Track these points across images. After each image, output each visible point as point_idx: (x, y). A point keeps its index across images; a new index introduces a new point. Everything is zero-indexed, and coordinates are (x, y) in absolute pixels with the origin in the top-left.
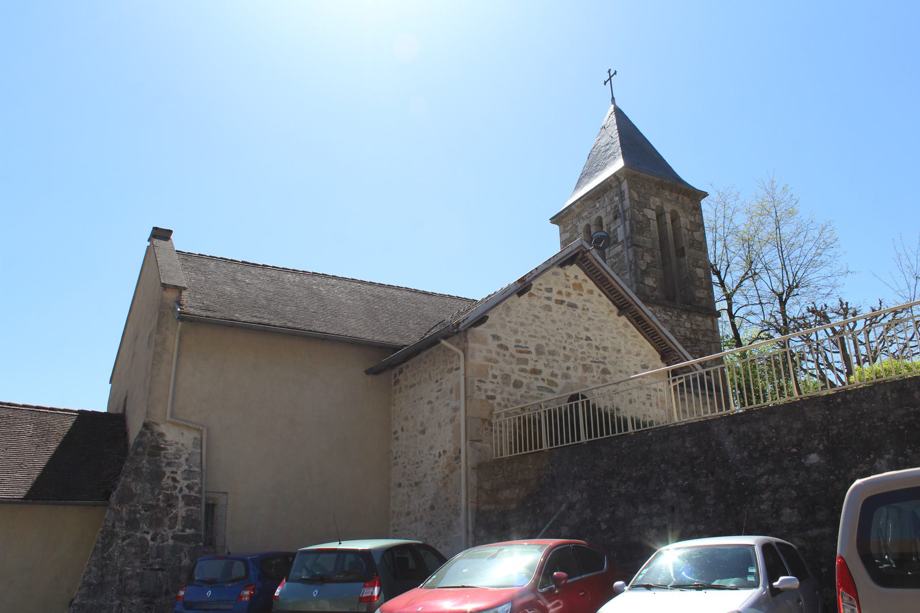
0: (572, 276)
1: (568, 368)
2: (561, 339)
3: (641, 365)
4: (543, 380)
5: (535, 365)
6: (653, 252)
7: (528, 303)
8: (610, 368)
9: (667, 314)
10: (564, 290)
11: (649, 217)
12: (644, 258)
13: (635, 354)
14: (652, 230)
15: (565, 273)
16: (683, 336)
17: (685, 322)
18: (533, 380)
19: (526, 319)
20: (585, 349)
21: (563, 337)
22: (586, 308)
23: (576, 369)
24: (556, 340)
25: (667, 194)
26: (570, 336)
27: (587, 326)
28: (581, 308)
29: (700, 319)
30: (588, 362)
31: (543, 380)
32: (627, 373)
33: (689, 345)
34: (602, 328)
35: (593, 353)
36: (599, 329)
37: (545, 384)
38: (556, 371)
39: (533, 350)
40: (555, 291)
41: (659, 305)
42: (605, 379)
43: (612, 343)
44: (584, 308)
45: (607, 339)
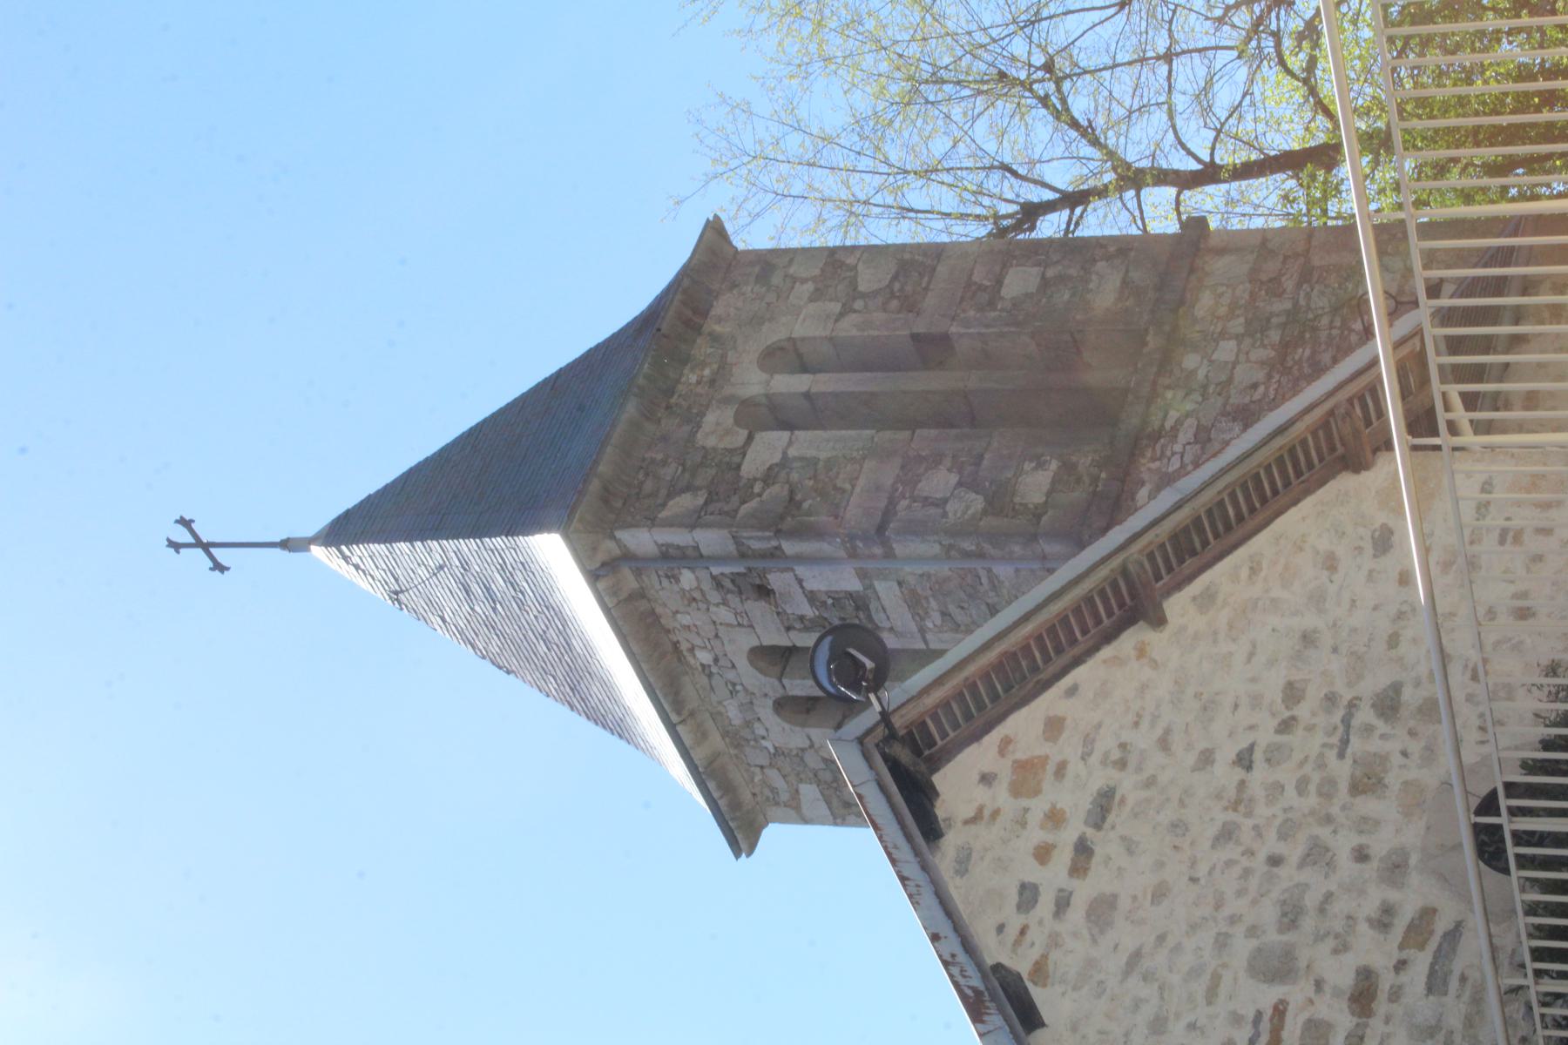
0: (981, 795)
1: (1361, 856)
2: (1236, 871)
3: (1375, 556)
4: (1401, 965)
5: (1337, 992)
7: (1075, 988)
8: (1375, 681)
10: (1037, 835)
13: (1326, 573)
15: (966, 822)
16: (1269, 377)
17: (1211, 362)
18: (1398, 1009)
19: (1137, 1005)
20: (1286, 774)
21: (1230, 863)
22: (1116, 755)
23: (1366, 824)
24: (1240, 893)
25: (693, 378)
26: (1227, 834)
27: (1191, 759)
28: (1114, 774)
29: (1205, 302)
30: (1342, 771)
31: (1401, 965)
32: (1400, 615)
33: (1308, 352)
34: (1205, 697)
35: (1306, 744)
36: (1208, 708)
37: (1421, 962)
38: (1370, 906)
39: (1268, 996)
40: (1032, 872)
42: (1420, 710)
43: (1272, 663)
44: (1115, 763)
45: (1254, 680)
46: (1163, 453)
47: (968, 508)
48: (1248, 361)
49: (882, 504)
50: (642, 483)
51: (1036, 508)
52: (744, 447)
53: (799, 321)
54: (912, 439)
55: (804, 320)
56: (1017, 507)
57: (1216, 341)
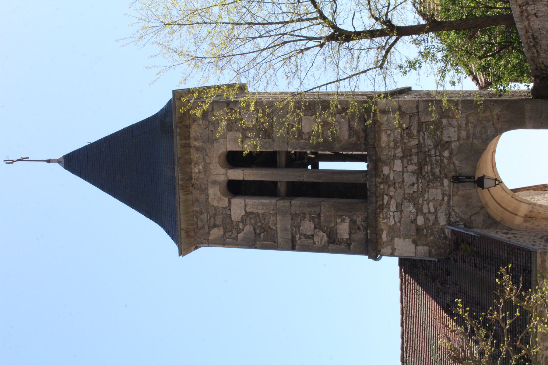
6: (296, 214)
9: (388, 204)
11: (243, 213)
12: (309, 233)
16: (418, 180)
17: (394, 171)
25: (197, 171)
29: (384, 138)
33: (429, 168)
41: (376, 221)
47: (322, 240)
48: (407, 172)
49: (290, 237)
50: (197, 222)
51: (347, 241)
54: (291, 206)
55: (229, 141)
56: (340, 240)
57: (393, 160)
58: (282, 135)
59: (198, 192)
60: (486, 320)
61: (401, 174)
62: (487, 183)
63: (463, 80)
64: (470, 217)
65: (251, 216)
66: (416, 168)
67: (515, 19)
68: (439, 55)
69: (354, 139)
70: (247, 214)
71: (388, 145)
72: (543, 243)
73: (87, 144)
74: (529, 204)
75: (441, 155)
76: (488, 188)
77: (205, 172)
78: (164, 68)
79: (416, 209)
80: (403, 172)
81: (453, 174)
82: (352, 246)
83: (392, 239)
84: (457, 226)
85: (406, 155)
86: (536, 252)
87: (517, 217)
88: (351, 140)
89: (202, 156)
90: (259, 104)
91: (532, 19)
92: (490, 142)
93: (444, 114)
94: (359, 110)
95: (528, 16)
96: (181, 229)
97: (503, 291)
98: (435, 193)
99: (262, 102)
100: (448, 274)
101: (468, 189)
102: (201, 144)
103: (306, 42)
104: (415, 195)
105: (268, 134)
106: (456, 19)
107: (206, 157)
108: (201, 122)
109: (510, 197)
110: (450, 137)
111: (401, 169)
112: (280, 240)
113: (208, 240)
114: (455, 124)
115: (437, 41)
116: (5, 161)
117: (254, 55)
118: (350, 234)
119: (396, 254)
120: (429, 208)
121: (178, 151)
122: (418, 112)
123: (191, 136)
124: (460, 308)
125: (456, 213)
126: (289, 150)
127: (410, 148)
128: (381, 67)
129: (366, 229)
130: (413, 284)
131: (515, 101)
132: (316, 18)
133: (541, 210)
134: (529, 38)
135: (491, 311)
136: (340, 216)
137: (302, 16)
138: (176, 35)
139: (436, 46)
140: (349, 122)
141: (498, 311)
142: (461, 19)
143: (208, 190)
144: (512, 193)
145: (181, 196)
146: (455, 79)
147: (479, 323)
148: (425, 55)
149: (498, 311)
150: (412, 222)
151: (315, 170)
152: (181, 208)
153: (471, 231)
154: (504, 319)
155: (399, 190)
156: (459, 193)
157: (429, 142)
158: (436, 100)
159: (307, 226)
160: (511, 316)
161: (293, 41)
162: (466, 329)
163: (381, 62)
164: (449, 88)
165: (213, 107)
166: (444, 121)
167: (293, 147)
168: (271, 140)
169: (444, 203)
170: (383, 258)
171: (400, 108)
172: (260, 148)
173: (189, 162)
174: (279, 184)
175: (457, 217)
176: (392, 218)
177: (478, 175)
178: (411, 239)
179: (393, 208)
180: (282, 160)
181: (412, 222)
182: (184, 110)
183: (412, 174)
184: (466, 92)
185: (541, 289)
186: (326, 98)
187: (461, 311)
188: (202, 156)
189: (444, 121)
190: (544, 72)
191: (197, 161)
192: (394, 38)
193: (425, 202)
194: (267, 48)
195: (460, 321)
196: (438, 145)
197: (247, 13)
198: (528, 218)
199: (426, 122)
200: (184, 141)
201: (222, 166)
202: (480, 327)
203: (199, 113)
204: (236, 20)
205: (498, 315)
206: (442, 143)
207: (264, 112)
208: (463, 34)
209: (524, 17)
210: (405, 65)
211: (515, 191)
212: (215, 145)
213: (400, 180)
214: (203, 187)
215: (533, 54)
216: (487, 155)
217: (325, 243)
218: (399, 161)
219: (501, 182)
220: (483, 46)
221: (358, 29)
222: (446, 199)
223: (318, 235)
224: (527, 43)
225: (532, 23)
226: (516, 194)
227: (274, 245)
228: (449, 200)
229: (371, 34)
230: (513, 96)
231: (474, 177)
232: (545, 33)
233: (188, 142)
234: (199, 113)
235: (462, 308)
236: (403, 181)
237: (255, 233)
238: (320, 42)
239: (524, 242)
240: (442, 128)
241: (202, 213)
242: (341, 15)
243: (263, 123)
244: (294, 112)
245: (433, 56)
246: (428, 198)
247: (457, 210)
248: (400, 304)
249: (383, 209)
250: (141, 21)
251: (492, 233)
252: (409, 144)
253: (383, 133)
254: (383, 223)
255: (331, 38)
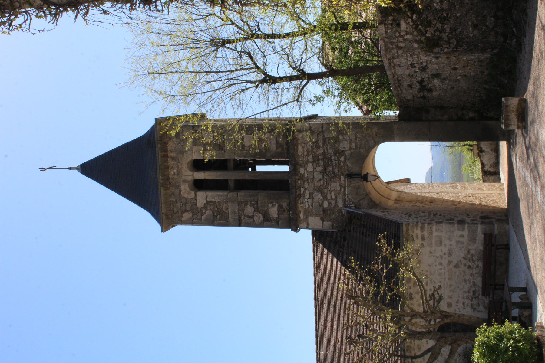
6: (241, 201)
9: (304, 193)
11: (205, 202)
14: (218, 200)
16: (323, 177)
25: (173, 173)
29: (300, 149)
33: (331, 169)
46: (303, 202)
50: (173, 208)
51: (276, 219)
52: (195, 197)
53: (193, 153)
54: (238, 196)
55: (194, 153)
57: (307, 164)
58: (230, 148)
59: (174, 188)
60: (370, 270)
61: (312, 173)
62: (370, 178)
63: (353, 109)
64: (359, 202)
65: (211, 204)
66: (322, 169)
67: (386, 68)
68: (336, 93)
69: (280, 150)
70: (208, 202)
71: (303, 154)
72: (407, 218)
73: (96, 156)
74: (398, 192)
75: (339, 160)
76: (370, 182)
77: (178, 174)
78: (149, 103)
79: (323, 197)
80: (313, 172)
81: (347, 172)
82: (280, 223)
83: (307, 218)
84: (350, 207)
85: (315, 161)
86: (402, 223)
87: (390, 201)
88: (278, 150)
89: (176, 163)
90: (214, 127)
91: (397, 68)
92: (371, 151)
93: (340, 132)
94: (283, 130)
95: (394, 66)
96: (162, 214)
97: (381, 251)
98: (335, 186)
99: (217, 125)
100: (345, 240)
101: (357, 182)
102: (175, 155)
103: (246, 84)
104: (321, 187)
105: (221, 147)
106: (347, 68)
107: (179, 164)
108: (174, 140)
109: (384, 187)
110: (344, 148)
111: (312, 170)
112: (231, 220)
113: (181, 220)
114: (348, 138)
115: (334, 83)
116: (39, 169)
117: (211, 93)
118: (278, 214)
119: (309, 227)
120: (331, 196)
121: (160, 160)
122: (323, 131)
123: (168, 149)
124: (353, 262)
125: (349, 199)
126: (236, 158)
127: (317, 155)
128: (297, 101)
129: (289, 211)
130: (322, 248)
131: (387, 123)
132: (252, 68)
133: (405, 196)
134: (395, 81)
135: (374, 264)
136: (272, 203)
137: (243, 66)
138: (157, 81)
139: (334, 86)
140: (276, 138)
141: (378, 264)
142: (350, 68)
143: (180, 187)
144: (386, 185)
145: (162, 191)
146: (347, 109)
147: (365, 273)
148: (327, 92)
149: (378, 264)
150: (320, 206)
151: (253, 171)
152: (162, 199)
153: (360, 211)
154: (382, 269)
155: (311, 184)
156: (352, 185)
157: (331, 151)
158: (335, 123)
159: (249, 210)
160: (387, 267)
161: (237, 84)
162: (357, 276)
163: (297, 97)
164: (343, 114)
165: (183, 130)
166: (341, 137)
167: (239, 156)
168: (223, 151)
169: (342, 192)
170: (301, 230)
171: (310, 129)
172: (216, 157)
173: (167, 167)
174: (229, 182)
175: (350, 201)
176: (306, 203)
177: (364, 173)
178: (320, 217)
179: (307, 196)
180: (231, 165)
181: (320, 206)
182: (163, 132)
183: (319, 173)
184: (355, 117)
185: (406, 248)
186: (261, 122)
187: (353, 265)
188: (176, 163)
189: (341, 137)
190: (406, 103)
191: (173, 166)
192: (306, 81)
193: (329, 192)
194: (219, 89)
195: (353, 271)
196: (336, 153)
197: (206, 65)
198: (397, 201)
199: (328, 138)
200: (163, 153)
201: (189, 170)
202: (367, 275)
203: (173, 134)
204: (198, 69)
205: (378, 267)
206: (339, 151)
207: (218, 132)
208: (352, 78)
209: (391, 67)
210: (313, 99)
211: (388, 183)
212: (185, 155)
213: (312, 177)
214: (177, 184)
215: (398, 91)
216: (369, 160)
217: (262, 221)
218: (311, 164)
219: (379, 177)
220: (365, 86)
221: (281, 75)
222: (342, 189)
223: (256, 216)
224: (394, 84)
225: (397, 71)
226: (389, 185)
227: (226, 224)
228: (345, 190)
229: (290, 78)
230: (386, 119)
231: (361, 175)
232: (405, 77)
233: (166, 153)
234: (173, 134)
235: (354, 262)
236: (314, 178)
237: (214, 215)
238: (256, 84)
239: (394, 217)
240: (339, 142)
241: (176, 203)
242: (270, 66)
243: (217, 140)
244: (238, 132)
245: (332, 93)
246: (331, 189)
247: (350, 197)
248: (313, 261)
249: (301, 197)
250: (132, 71)
251: (375, 212)
252: (317, 153)
253: (300, 146)
254: (300, 206)
255: (263, 81)
